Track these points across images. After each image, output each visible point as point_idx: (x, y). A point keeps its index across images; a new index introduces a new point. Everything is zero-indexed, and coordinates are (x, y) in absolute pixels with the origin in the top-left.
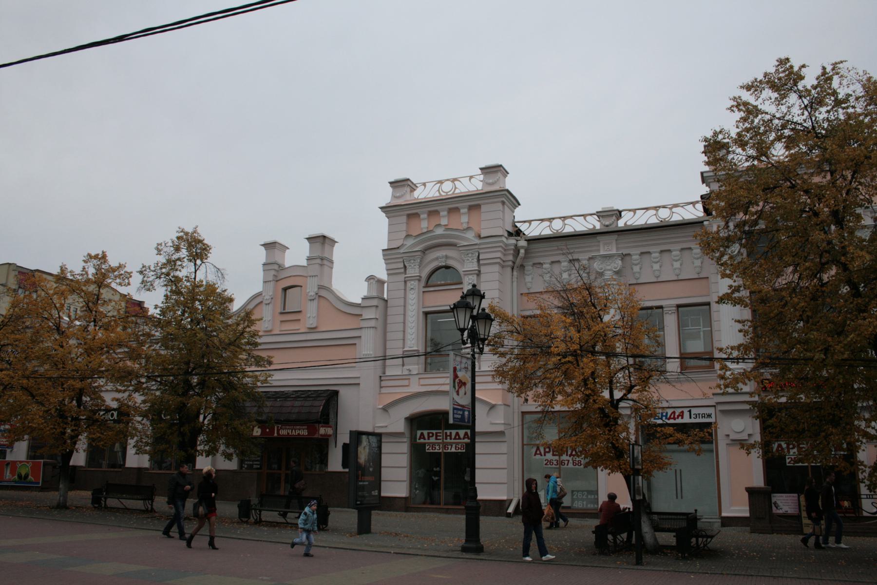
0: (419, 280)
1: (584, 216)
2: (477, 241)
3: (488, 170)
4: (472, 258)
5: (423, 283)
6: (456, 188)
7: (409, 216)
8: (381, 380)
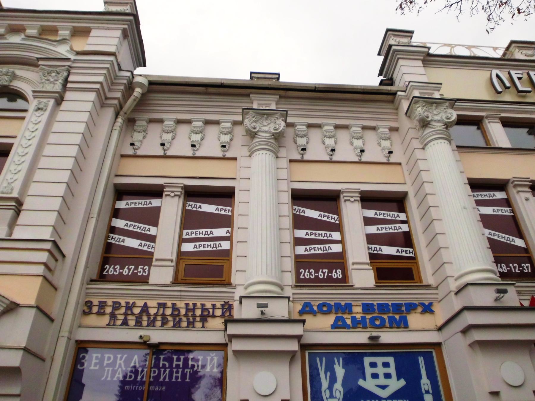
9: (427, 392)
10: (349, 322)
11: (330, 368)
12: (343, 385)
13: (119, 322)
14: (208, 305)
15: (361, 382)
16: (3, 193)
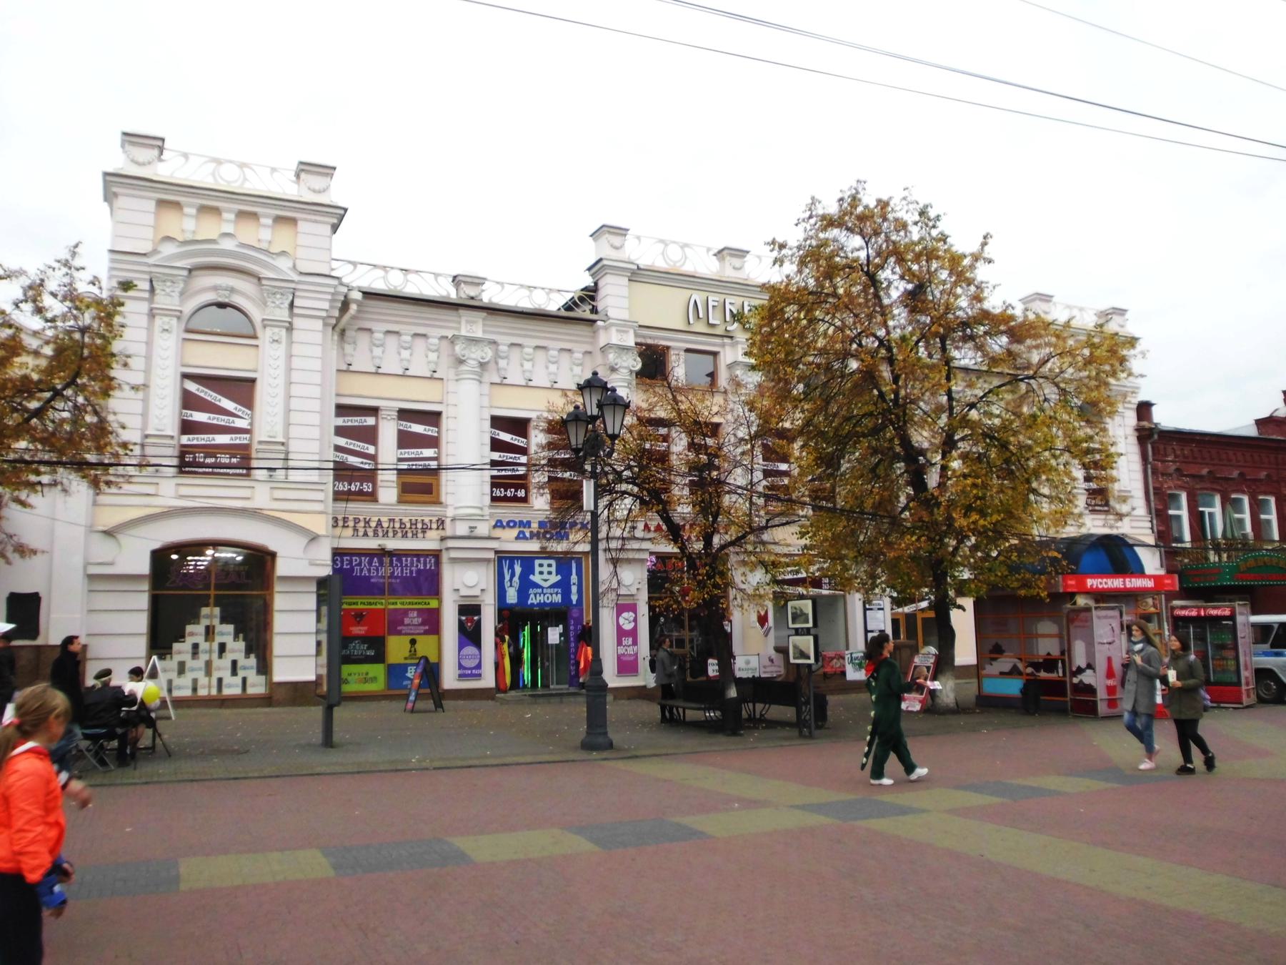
0: (179, 318)
1: (436, 275)
2: (296, 277)
3: (305, 168)
4: (280, 301)
6: (245, 179)
7: (161, 203)
9: (574, 584)
10: (528, 535)
11: (511, 567)
12: (520, 578)
13: (361, 533)
14: (427, 520)
15: (531, 577)
16: (271, 437)
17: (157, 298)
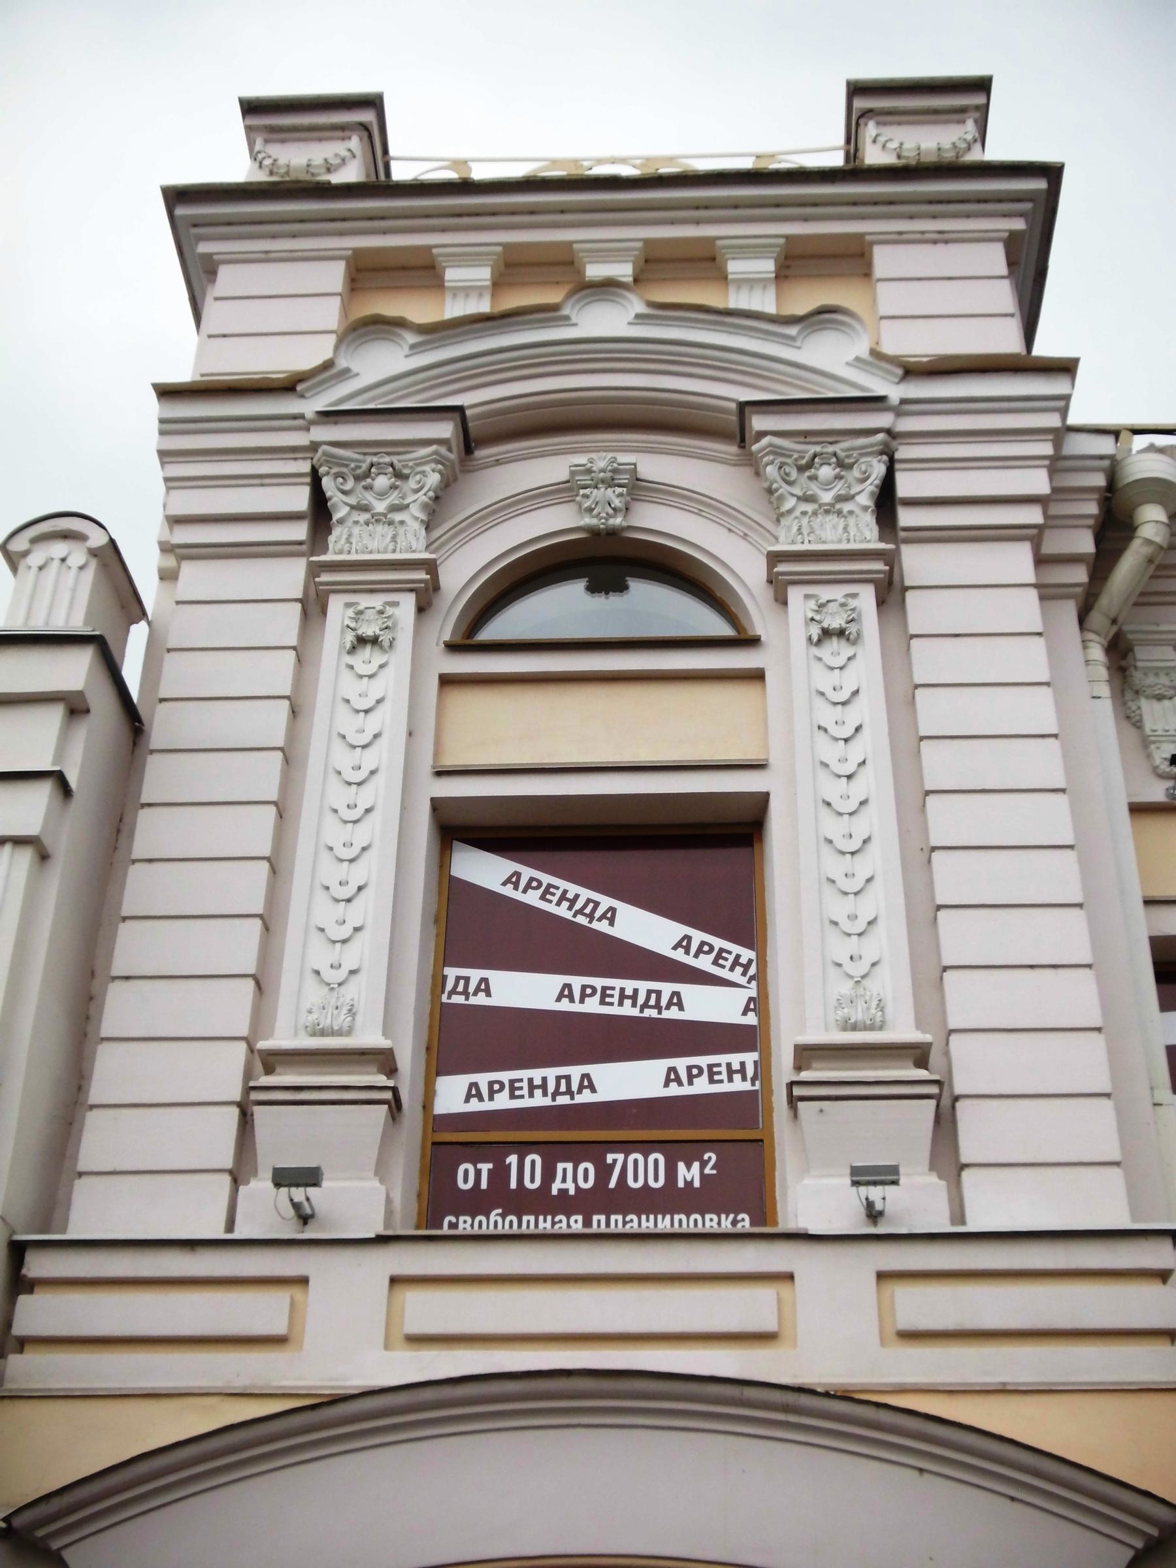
4: (839, 488)
5: (445, 626)
8: (20, 1284)
17: (336, 538)
